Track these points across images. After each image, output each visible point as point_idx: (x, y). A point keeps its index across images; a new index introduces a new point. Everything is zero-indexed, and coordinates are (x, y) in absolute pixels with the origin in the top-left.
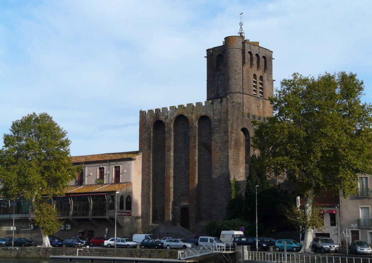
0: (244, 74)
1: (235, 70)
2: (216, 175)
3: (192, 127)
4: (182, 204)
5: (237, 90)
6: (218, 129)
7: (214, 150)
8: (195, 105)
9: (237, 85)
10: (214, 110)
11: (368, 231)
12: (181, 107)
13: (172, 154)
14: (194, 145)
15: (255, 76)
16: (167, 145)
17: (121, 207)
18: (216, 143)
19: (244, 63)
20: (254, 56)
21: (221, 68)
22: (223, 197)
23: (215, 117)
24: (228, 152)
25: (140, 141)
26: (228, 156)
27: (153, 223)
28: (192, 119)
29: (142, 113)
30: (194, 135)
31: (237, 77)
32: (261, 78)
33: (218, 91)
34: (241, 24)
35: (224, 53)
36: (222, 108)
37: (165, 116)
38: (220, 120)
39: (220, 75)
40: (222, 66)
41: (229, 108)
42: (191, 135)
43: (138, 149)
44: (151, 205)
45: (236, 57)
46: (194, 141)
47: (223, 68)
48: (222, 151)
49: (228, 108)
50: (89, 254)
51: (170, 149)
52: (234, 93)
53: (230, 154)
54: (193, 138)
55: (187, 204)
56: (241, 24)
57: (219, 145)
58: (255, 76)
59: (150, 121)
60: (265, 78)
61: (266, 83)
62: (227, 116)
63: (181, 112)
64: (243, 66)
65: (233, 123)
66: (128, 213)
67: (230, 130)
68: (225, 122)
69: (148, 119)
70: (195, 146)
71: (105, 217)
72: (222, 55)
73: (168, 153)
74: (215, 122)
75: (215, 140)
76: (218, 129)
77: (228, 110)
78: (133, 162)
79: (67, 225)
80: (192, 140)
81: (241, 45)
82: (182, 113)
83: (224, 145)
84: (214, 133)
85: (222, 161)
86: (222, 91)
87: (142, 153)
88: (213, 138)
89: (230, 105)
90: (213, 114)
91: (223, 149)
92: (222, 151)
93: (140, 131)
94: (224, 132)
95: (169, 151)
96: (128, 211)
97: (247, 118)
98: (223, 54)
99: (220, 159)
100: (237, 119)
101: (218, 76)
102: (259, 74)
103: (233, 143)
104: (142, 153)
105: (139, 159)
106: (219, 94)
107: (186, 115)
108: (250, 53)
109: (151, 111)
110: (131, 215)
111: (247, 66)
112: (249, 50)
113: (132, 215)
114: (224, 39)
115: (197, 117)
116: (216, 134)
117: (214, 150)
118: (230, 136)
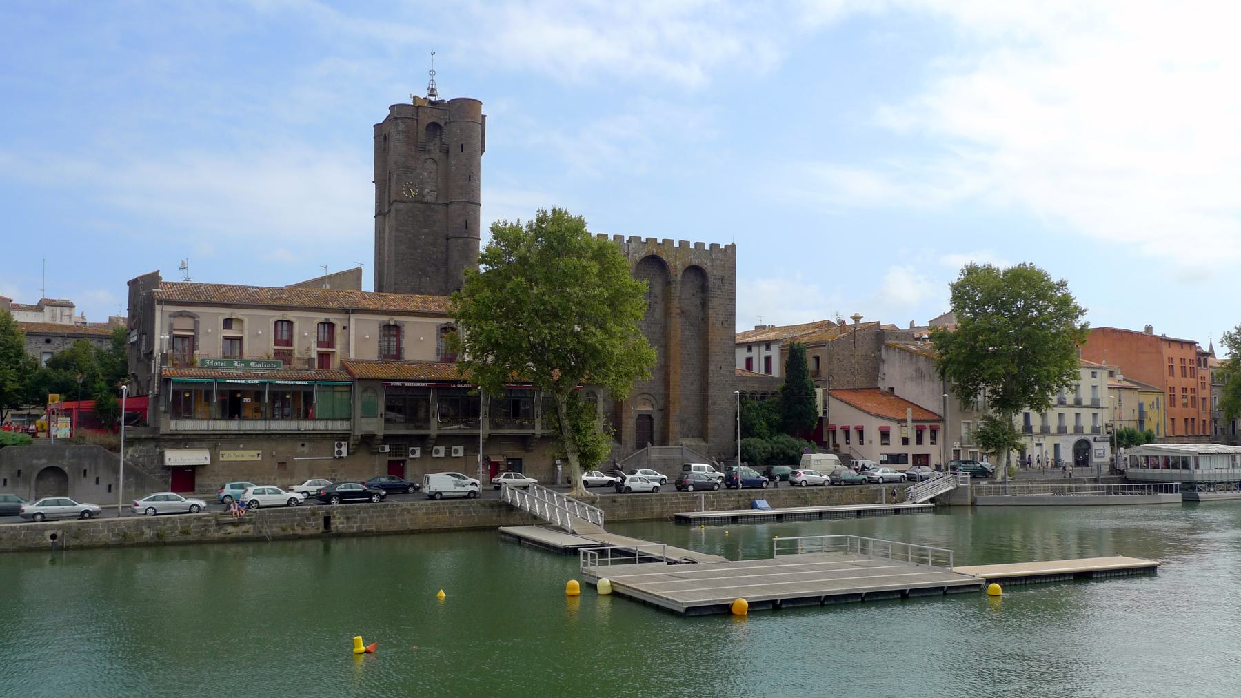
2: (716, 365)
3: (675, 281)
6: (719, 292)
8: (676, 245)
10: (712, 260)
11: (969, 450)
12: (699, 245)
18: (716, 314)
21: (432, 148)
22: (726, 401)
23: (715, 273)
28: (675, 266)
33: (422, 189)
34: (432, 73)
36: (727, 260)
37: (624, 251)
39: (428, 161)
40: (434, 145)
42: (674, 293)
47: (434, 149)
48: (725, 328)
50: (713, 502)
54: (677, 299)
55: (650, 409)
56: (432, 73)
63: (655, 251)
68: (730, 283)
74: (715, 279)
75: (713, 309)
79: (435, 448)
82: (657, 253)
84: (713, 297)
85: (724, 343)
86: (431, 191)
90: (712, 266)
91: (726, 326)
92: (725, 328)
94: (730, 299)
99: (722, 339)
107: (664, 258)
115: (683, 266)
116: (715, 299)
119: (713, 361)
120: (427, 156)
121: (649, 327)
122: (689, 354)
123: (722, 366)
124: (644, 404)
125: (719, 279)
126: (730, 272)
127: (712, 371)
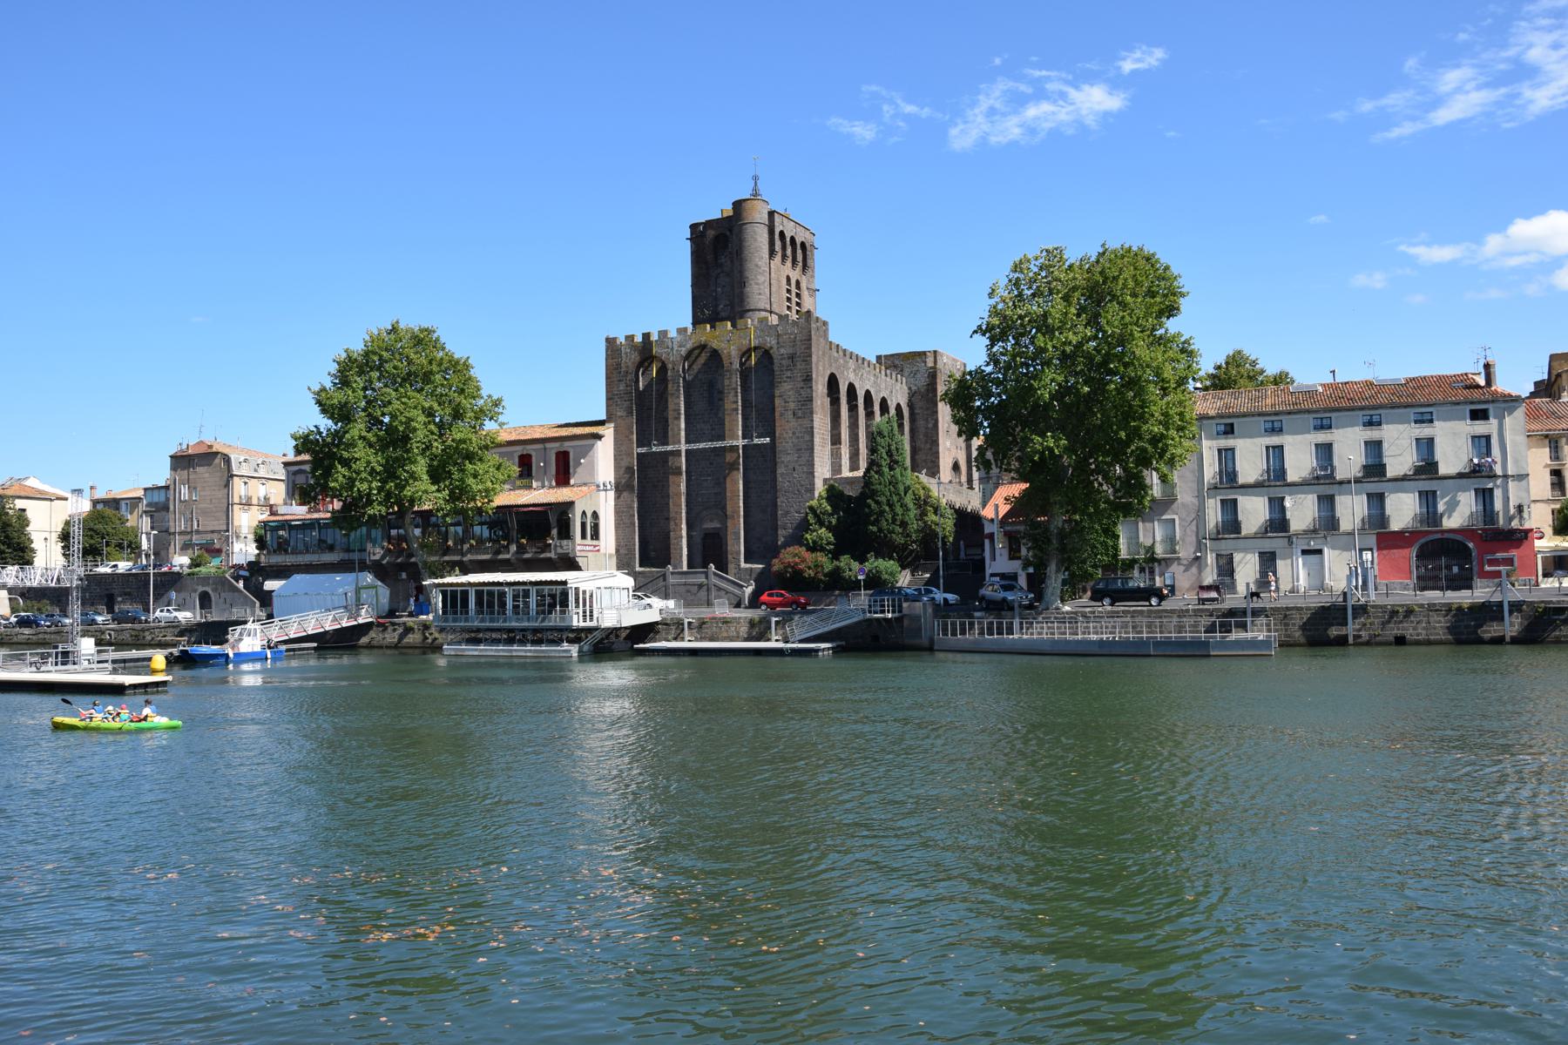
0: (773, 274)
1: (757, 266)
4: (705, 526)
5: (764, 304)
6: (789, 374)
7: (781, 415)
9: (760, 294)
13: (683, 426)
14: (735, 406)
15: (788, 279)
16: (671, 406)
17: (584, 536)
19: (772, 253)
20: (788, 240)
23: (782, 351)
24: (812, 421)
25: (608, 399)
26: (812, 428)
27: (640, 566)
29: (610, 342)
30: (734, 386)
31: (761, 279)
32: (798, 283)
33: (717, 306)
34: (756, 178)
35: (730, 231)
38: (792, 357)
41: (813, 333)
43: (603, 417)
44: (637, 529)
45: (758, 239)
46: (735, 399)
49: (810, 332)
51: (679, 414)
52: (752, 310)
53: (816, 424)
55: (718, 526)
56: (756, 178)
57: (792, 405)
58: (788, 279)
59: (630, 359)
60: (803, 285)
61: (805, 293)
62: (809, 347)
64: (770, 259)
65: (818, 361)
66: (595, 546)
67: (814, 376)
69: (626, 353)
70: (737, 409)
71: (548, 555)
72: (725, 236)
73: (676, 422)
76: (789, 374)
77: (810, 336)
78: (599, 442)
80: (731, 397)
81: (767, 216)
83: (802, 405)
85: (798, 437)
87: (612, 425)
88: (777, 393)
89: (813, 326)
93: (607, 378)
94: (804, 380)
95: (678, 418)
96: (595, 542)
97: (836, 354)
98: (728, 233)
99: (794, 433)
100: (824, 354)
101: (716, 278)
102: (795, 275)
103: (819, 402)
104: (612, 425)
105: (608, 432)
106: (718, 314)
108: (782, 234)
109: (630, 338)
110: (598, 550)
111: (778, 258)
112: (781, 228)
113: (602, 551)
114: (733, 204)
115: (740, 350)
117: (781, 415)
118: (814, 388)
119: (783, 462)
120: (719, 271)
121: (712, 429)
122: (763, 456)
123: (797, 467)
124: (711, 521)
125: (789, 358)
126: (803, 347)
127: (782, 474)
